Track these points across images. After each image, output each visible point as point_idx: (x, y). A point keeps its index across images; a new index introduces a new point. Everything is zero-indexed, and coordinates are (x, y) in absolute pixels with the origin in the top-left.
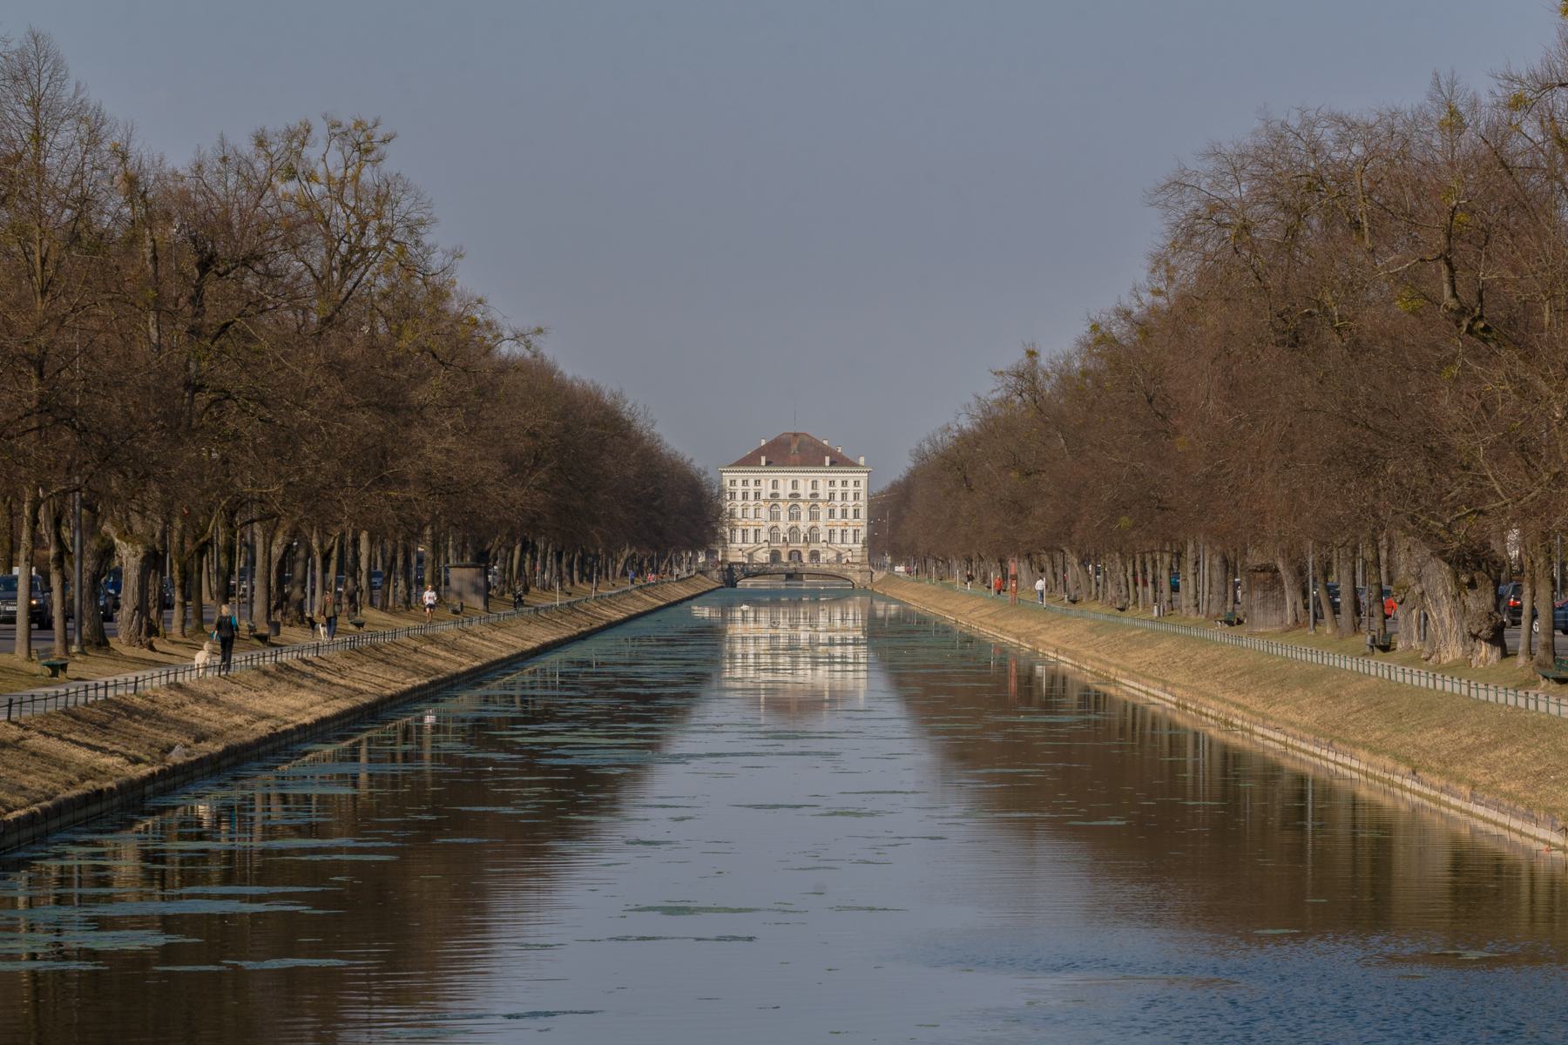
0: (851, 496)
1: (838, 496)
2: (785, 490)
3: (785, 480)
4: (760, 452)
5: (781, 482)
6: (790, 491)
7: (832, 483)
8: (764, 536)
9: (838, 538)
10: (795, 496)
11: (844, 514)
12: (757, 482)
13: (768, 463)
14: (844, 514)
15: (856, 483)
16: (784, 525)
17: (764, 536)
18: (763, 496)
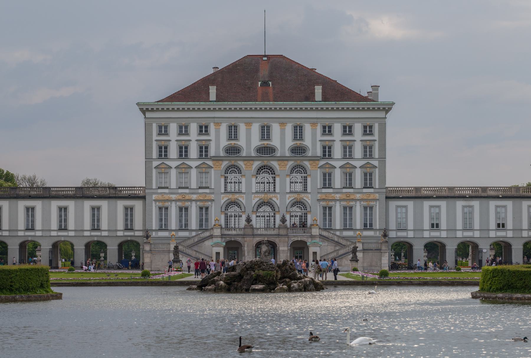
0: (358, 152)
2: (250, 139)
4: (206, 82)
5: (242, 129)
6: (256, 142)
7: (327, 130)
8: (216, 216)
9: (338, 223)
10: (266, 151)
12: (203, 130)
13: (220, 98)
15: (368, 130)
18: (212, 152)
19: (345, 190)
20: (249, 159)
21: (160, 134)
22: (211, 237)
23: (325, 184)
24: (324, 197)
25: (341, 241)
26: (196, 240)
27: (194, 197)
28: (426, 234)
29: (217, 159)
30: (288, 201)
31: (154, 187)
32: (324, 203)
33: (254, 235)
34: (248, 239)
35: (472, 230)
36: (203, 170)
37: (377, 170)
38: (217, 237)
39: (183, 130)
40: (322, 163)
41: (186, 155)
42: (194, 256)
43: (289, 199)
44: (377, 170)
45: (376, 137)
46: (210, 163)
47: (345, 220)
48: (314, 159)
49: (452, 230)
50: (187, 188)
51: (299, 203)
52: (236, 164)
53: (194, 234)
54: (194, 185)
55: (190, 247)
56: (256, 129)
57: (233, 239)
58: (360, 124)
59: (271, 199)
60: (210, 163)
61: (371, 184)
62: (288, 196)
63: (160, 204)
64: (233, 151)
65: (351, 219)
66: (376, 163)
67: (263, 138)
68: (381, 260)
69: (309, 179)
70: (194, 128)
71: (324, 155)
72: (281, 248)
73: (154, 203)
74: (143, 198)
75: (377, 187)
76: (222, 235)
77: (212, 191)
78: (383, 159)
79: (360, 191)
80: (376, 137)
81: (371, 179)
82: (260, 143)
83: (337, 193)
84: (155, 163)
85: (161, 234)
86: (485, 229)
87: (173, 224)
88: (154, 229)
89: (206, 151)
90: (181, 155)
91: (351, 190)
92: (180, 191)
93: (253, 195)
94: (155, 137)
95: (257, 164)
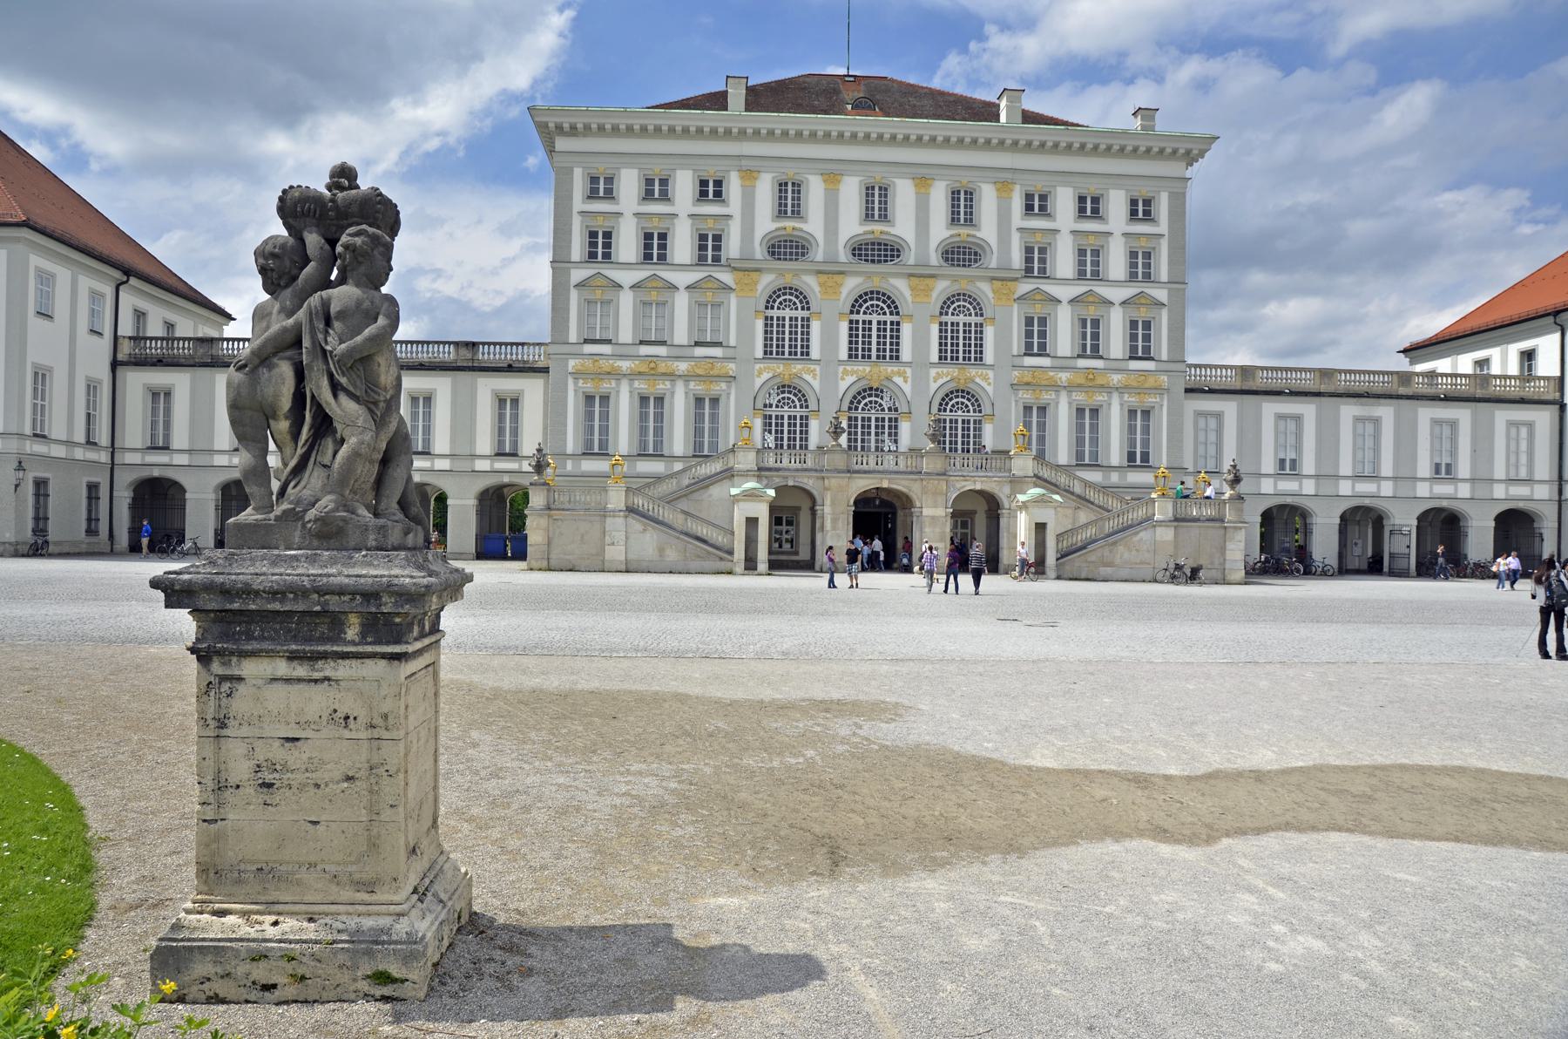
0: (1116, 263)
1: (1064, 261)
2: (831, 218)
3: (832, 177)
5: (815, 191)
6: (852, 225)
7: (1037, 204)
11: (1091, 340)
12: (709, 190)
14: (1091, 340)
15: (1141, 210)
16: (830, 375)
17: (740, 422)
18: (733, 247)
19: (1082, 363)
20: (831, 272)
21: (593, 195)
22: (728, 474)
23: (1029, 346)
24: (1028, 379)
25: (1091, 494)
26: (686, 482)
27: (683, 367)
28: (1267, 486)
29: (745, 268)
30: (934, 386)
31: (573, 337)
32: (1026, 396)
34: (833, 482)
35: (1375, 477)
36: (707, 297)
37: (1165, 314)
38: (745, 474)
39: (656, 189)
40: (1025, 287)
41: (662, 257)
42: (680, 528)
43: (940, 378)
44: (1165, 314)
46: (726, 277)
47: (1080, 441)
48: (1002, 278)
49: (1326, 476)
50: (663, 343)
51: (960, 395)
52: (795, 283)
53: (678, 466)
54: (681, 335)
55: (671, 500)
56: (851, 192)
57: (791, 483)
59: (888, 379)
60: (726, 277)
61: (1147, 349)
62: (933, 372)
63: (589, 386)
64: (787, 248)
65: (1095, 441)
66: (1161, 294)
67: (868, 216)
68: (1223, 550)
69: (989, 333)
70: (684, 185)
71: (1029, 270)
72: (926, 512)
73: (570, 381)
74: (545, 370)
75: (1164, 357)
76: (759, 469)
77: (730, 353)
78: (1177, 282)
79: (1122, 365)
80: (1163, 227)
81: (1147, 338)
82: (860, 230)
83: (1062, 368)
84: (577, 275)
85: (589, 465)
86: (1405, 478)
87: (623, 439)
88: (570, 450)
89: (717, 248)
90: (648, 257)
91: (1098, 364)
92: (645, 350)
93: (841, 369)
94: (578, 203)
95: (851, 286)
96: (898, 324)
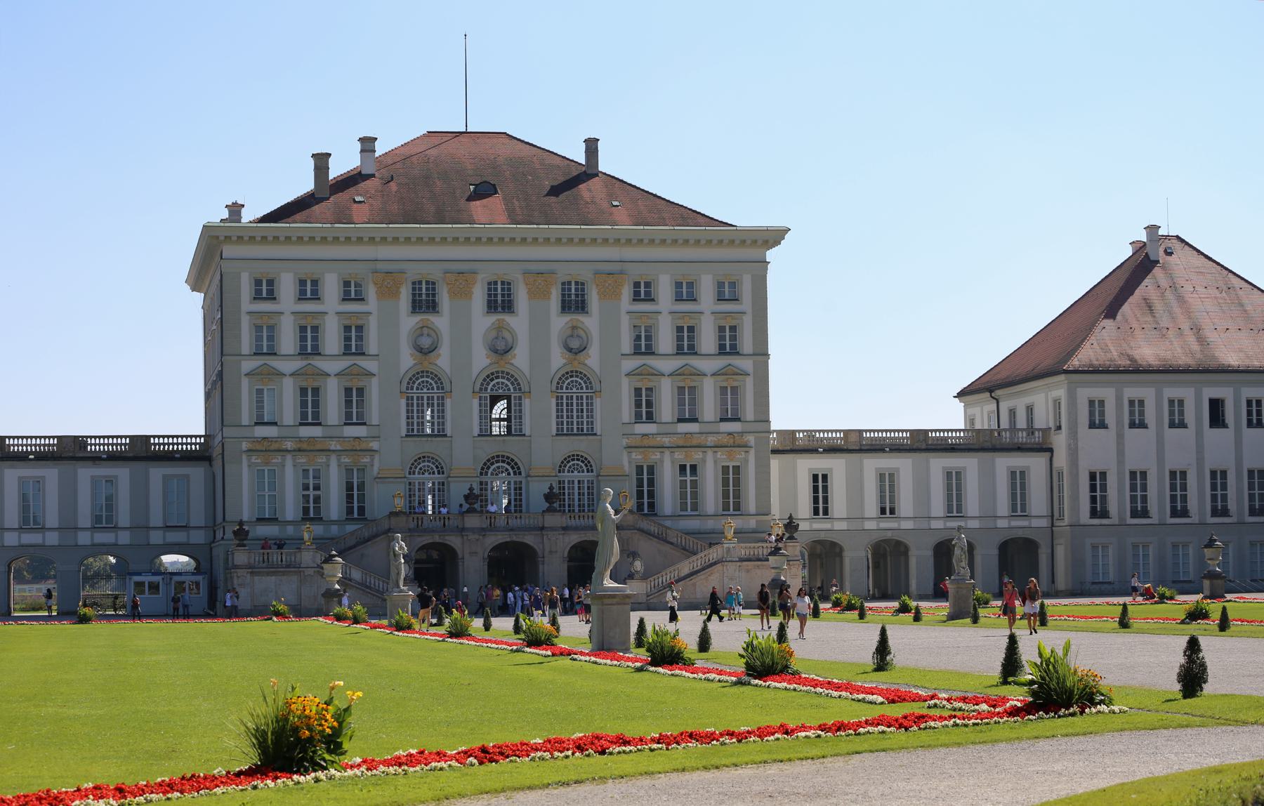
21: (257, 297)
31: (245, 421)
33: (482, 531)
37: (749, 382)
39: (309, 290)
44: (749, 382)
45: (746, 303)
58: (710, 277)
69: (597, 402)
73: (244, 457)
78: (762, 354)
84: (248, 365)
94: (247, 304)
96: (520, 398)
